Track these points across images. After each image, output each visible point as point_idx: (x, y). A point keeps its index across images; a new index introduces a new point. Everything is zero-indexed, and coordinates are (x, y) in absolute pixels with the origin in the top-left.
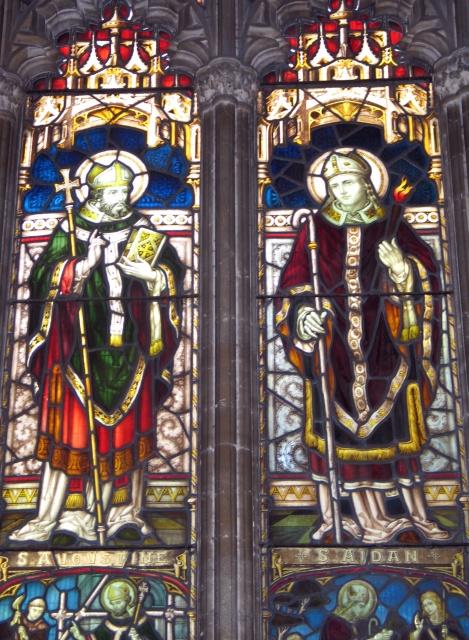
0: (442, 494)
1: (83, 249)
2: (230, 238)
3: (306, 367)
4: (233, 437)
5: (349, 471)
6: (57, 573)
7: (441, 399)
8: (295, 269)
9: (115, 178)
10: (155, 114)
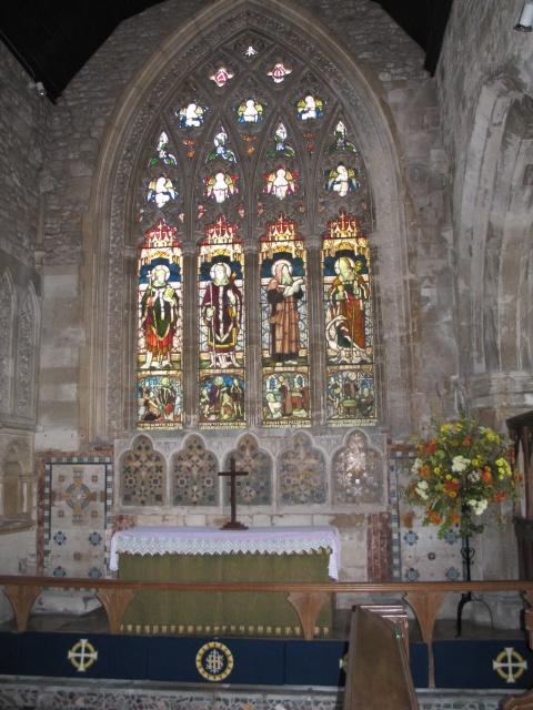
0: (240, 356)
1: (154, 293)
2: (191, 290)
3: (209, 324)
6: (151, 376)
7: (241, 332)
8: (207, 298)
9: (161, 273)
10: (172, 254)
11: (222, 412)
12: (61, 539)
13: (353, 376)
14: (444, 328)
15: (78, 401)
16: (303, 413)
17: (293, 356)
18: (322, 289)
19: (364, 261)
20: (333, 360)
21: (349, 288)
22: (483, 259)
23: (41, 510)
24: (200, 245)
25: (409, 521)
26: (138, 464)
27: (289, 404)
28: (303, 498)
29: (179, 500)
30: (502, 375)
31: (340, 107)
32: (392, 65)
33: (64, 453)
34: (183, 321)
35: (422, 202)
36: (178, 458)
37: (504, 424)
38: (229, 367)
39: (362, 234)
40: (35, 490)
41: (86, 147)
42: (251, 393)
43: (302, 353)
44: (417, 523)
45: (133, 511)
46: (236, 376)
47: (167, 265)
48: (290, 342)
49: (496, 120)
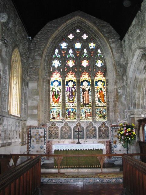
0: (75, 104)
2: (63, 88)
4: (64, 101)
5: (70, 102)
9: (56, 84)
11: (71, 117)
12: (33, 147)
13: (101, 109)
14: (123, 99)
15: (38, 114)
16: (90, 118)
17: (88, 104)
18: (94, 89)
19: (104, 83)
20: (97, 105)
21: (101, 89)
22: (133, 84)
23: (28, 140)
24: (66, 77)
25: (115, 142)
26: (52, 129)
27: (87, 116)
28: (91, 137)
29: (63, 137)
30: (137, 110)
31: (99, 46)
32: (112, 38)
33: (34, 127)
34: (62, 95)
35: (118, 70)
36: (62, 128)
37: (137, 121)
38: (73, 107)
39: (104, 76)
40: (27, 135)
41: (39, 52)
42: (78, 113)
43: (90, 104)
44: (117, 142)
45: (52, 140)
46: (75, 109)
47: (58, 82)
48: (87, 101)
49: (139, 56)
